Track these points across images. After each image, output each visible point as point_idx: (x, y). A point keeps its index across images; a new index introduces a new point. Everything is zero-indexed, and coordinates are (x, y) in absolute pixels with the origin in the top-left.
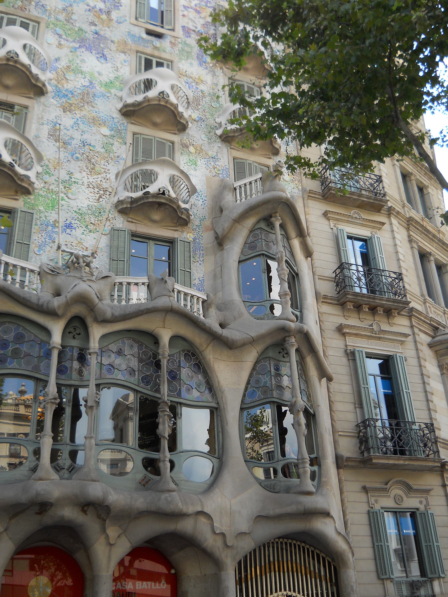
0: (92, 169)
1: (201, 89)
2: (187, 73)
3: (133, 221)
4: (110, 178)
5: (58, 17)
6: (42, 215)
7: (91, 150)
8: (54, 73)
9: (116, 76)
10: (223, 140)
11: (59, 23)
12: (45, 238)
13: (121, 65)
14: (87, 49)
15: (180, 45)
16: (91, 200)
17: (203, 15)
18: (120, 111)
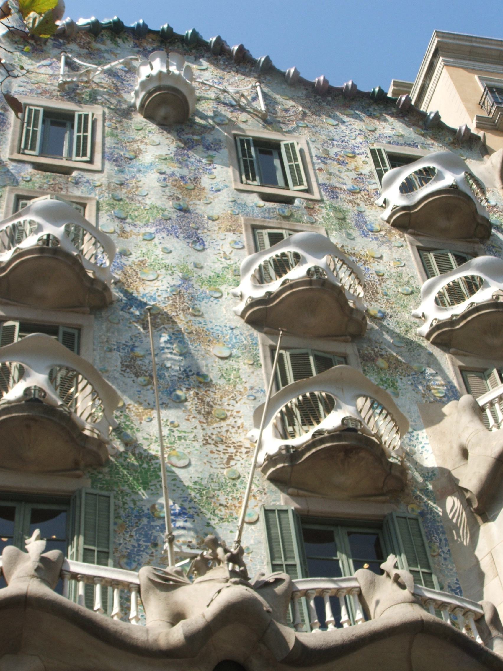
0: (209, 413)
1: (373, 269)
2: (345, 248)
3: (301, 492)
4: (242, 424)
5: (115, 193)
6: (128, 499)
7: (200, 382)
8: (119, 272)
9: (225, 265)
10: (433, 343)
11: (117, 202)
12: (138, 540)
13: (231, 249)
14: (169, 233)
15: (324, 211)
16: (214, 465)
17: (352, 166)
18: (242, 316)
